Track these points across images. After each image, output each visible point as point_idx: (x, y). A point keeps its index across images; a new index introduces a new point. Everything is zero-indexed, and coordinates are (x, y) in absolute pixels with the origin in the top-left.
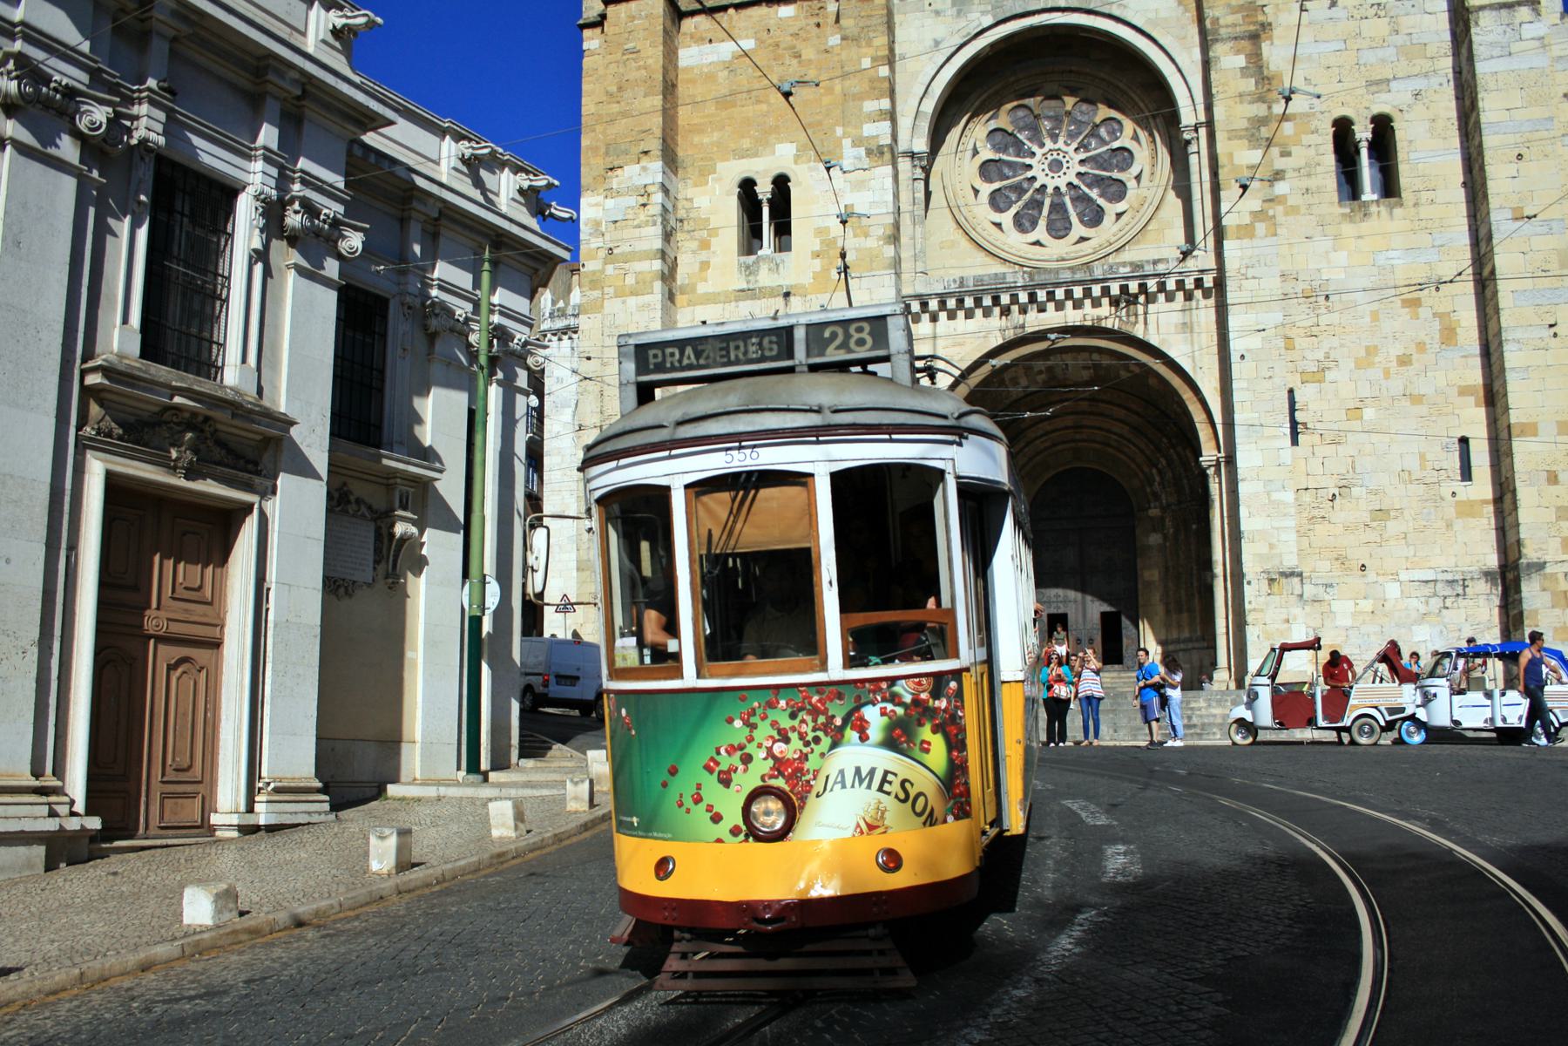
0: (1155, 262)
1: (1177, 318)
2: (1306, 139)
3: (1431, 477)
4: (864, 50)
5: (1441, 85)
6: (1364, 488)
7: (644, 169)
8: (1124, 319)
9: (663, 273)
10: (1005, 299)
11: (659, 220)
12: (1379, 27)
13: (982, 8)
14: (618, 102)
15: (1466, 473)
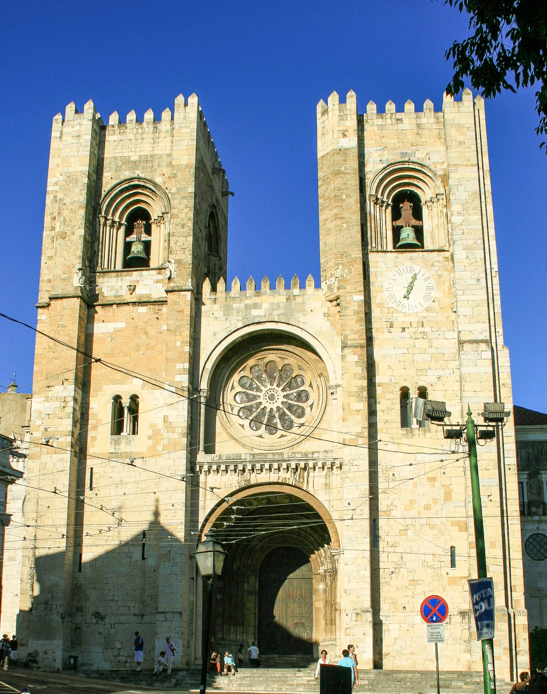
0: (313, 453)
1: (323, 481)
2: (388, 396)
3: (437, 565)
4: (178, 337)
5: (450, 374)
6: (406, 569)
7: (65, 388)
8: (298, 480)
9: (72, 443)
10: (240, 467)
11: (72, 416)
12: (422, 344)
13: (238, 318)
14: (54, 352)
15: (453, 565)
